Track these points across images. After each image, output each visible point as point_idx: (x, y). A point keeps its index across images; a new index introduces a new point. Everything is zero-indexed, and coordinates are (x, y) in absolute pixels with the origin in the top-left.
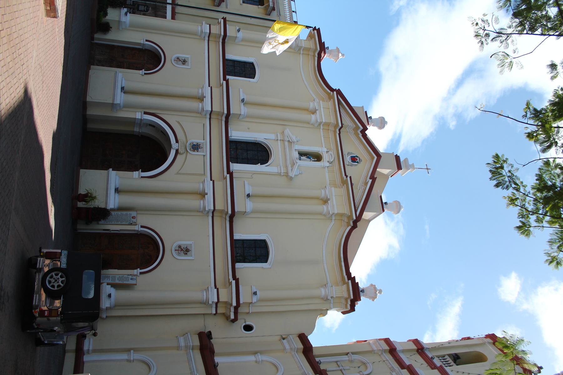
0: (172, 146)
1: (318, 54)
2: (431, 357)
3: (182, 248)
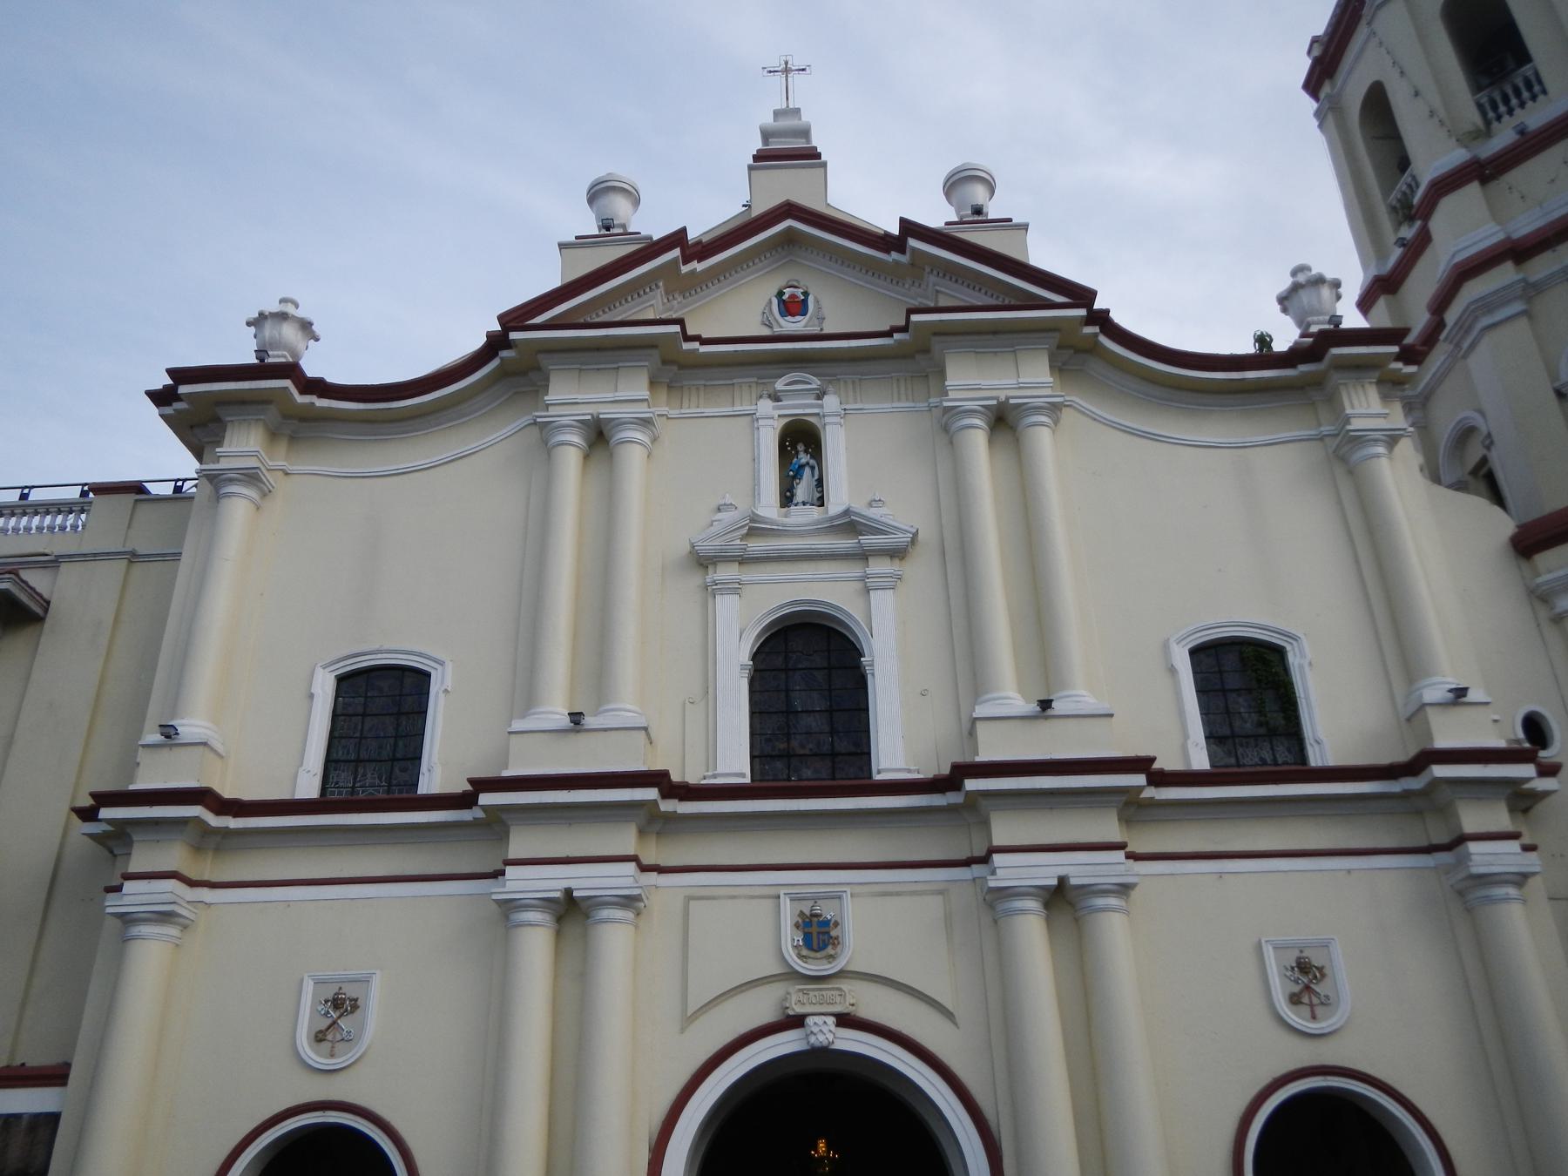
0: (817, 1044)
1: (302, 392)
2: (1517, 137)
3: (1296, 989)
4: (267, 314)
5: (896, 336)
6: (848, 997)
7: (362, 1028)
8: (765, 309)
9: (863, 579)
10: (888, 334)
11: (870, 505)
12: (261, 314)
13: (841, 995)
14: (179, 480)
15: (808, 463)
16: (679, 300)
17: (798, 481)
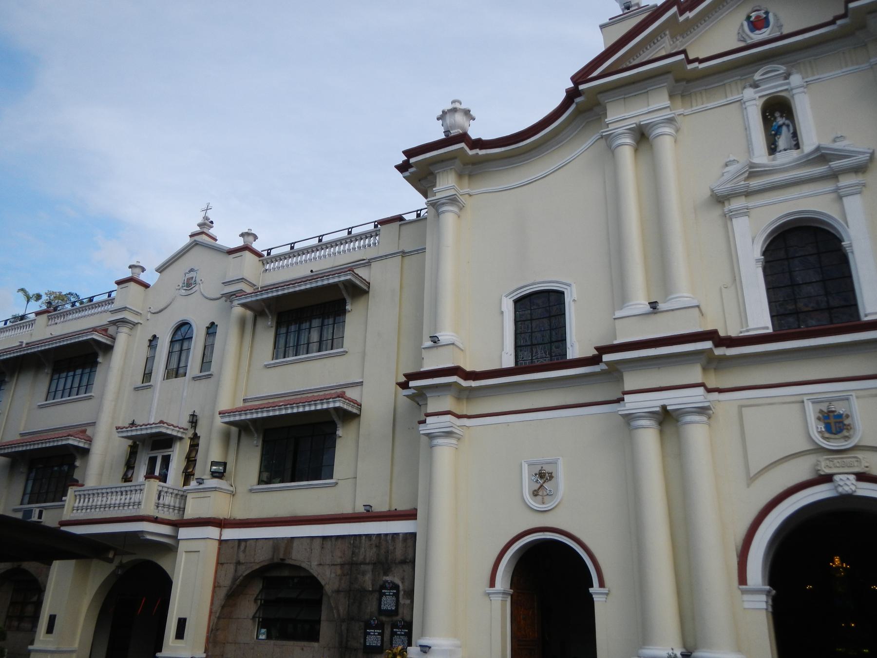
0: (844, 492)
1: (471, 148)
4: (446, 111)
5: (839, 22)
6: (863, 462)
8: (739, 30)
9: (836, 190)
10: (832, 22)
11: (834, 141)
12: (443, 112)
13: (857, 461)
14: (418, 210)
15: (784, 124)
16: (680, 40)
17: (778, 136)
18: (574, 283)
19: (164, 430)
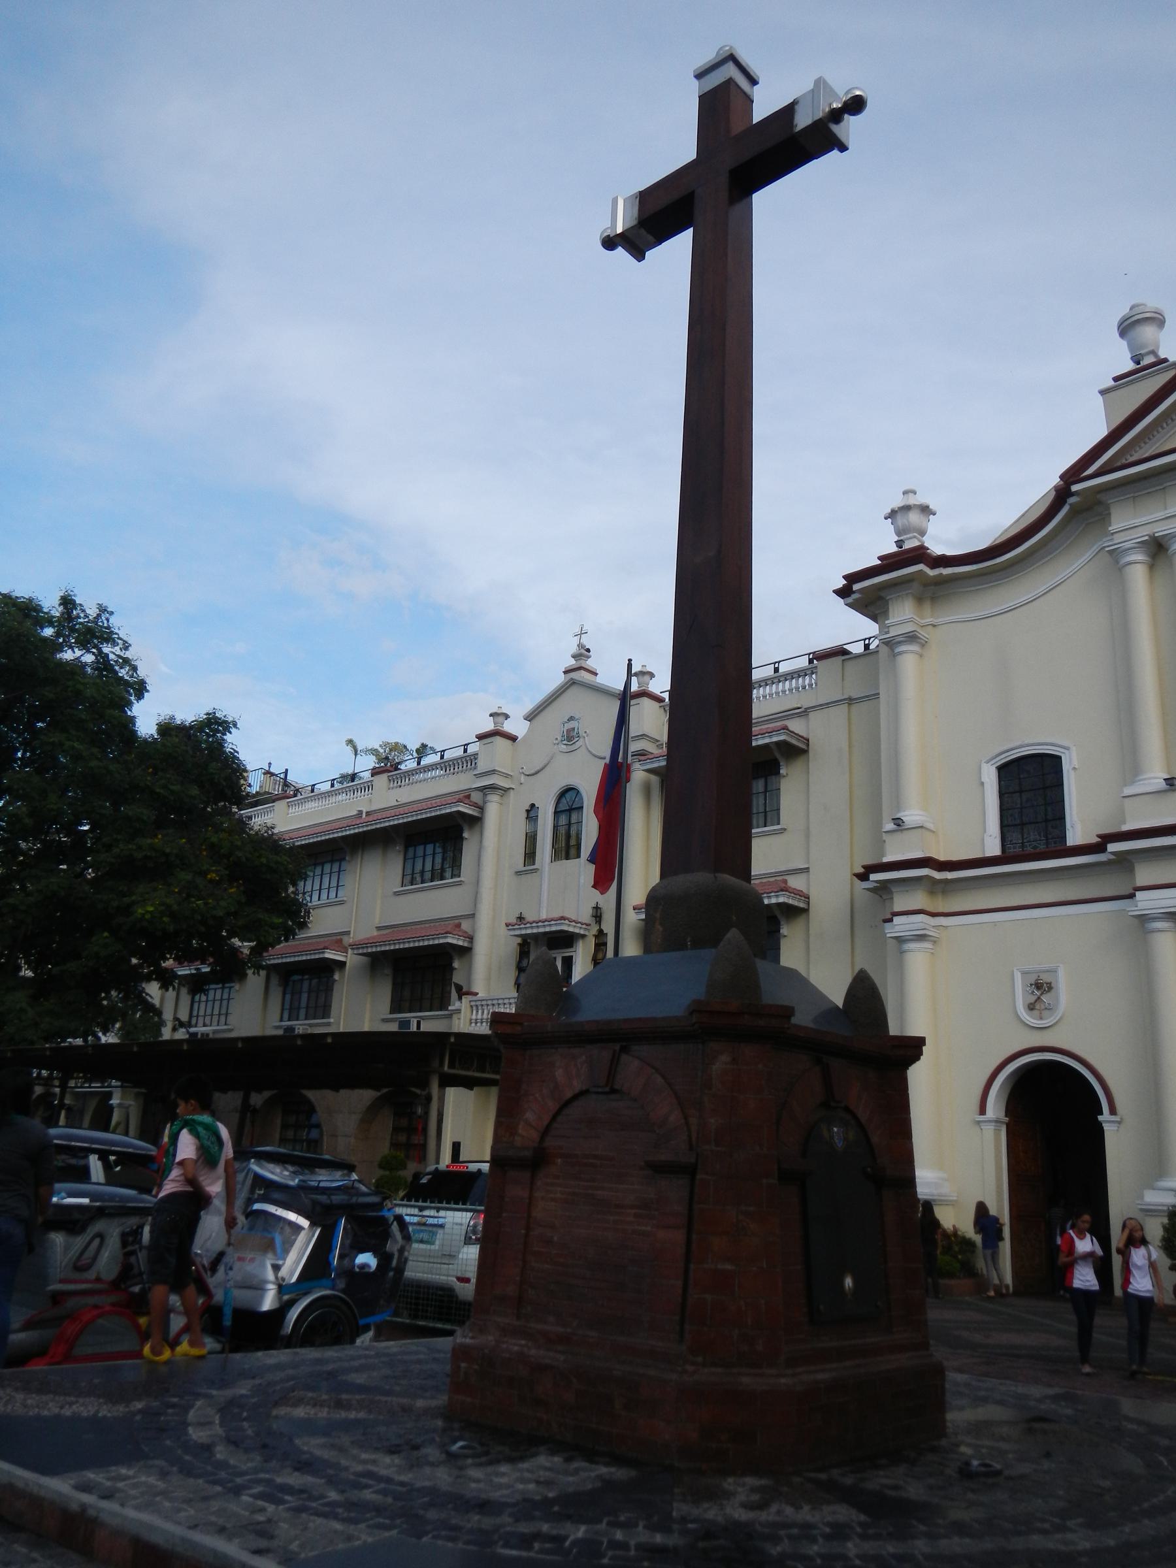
1: (933, 567)
4: (897, 509)
7: (1057, 999)
14: (866, 639)
18: (1075, 745)
19: (565, 928)
